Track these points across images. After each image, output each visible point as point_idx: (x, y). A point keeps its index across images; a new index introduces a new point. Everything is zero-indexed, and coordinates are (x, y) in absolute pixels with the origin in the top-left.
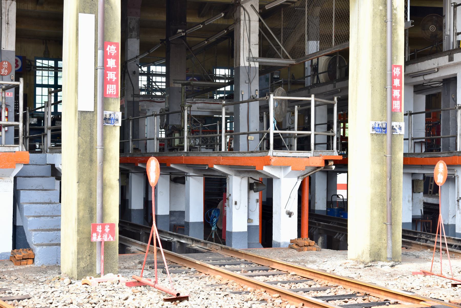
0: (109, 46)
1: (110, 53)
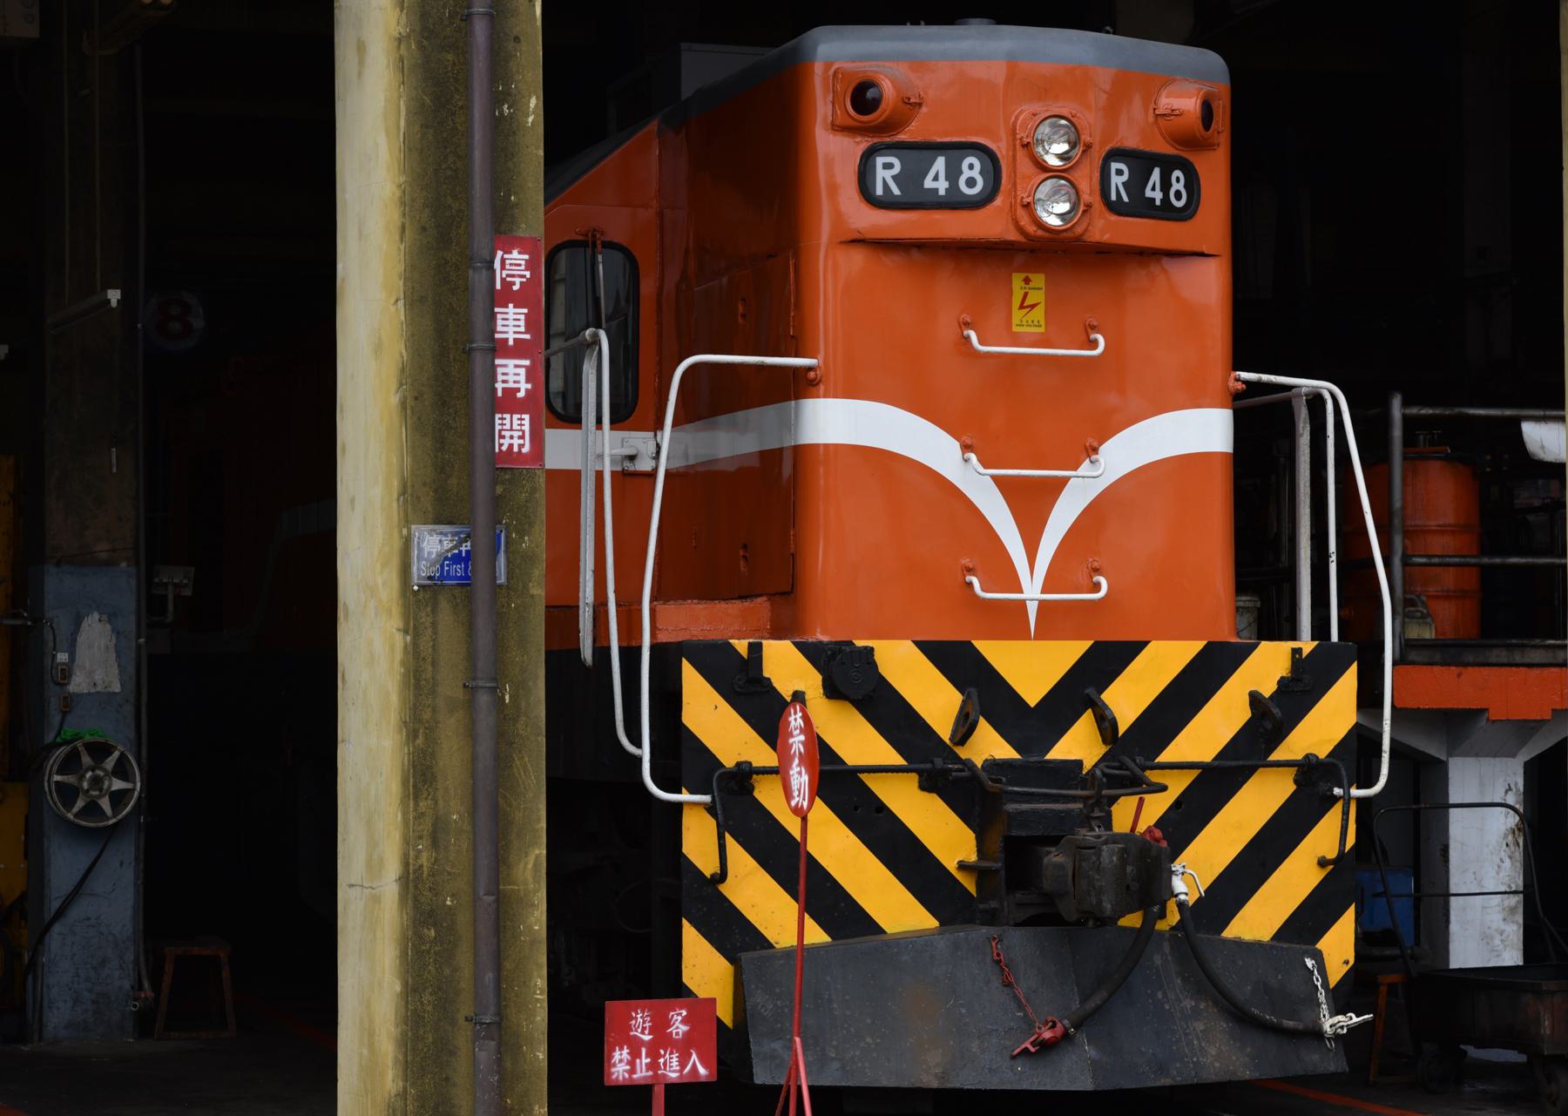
0: (500, 253)
1: (503, 280)
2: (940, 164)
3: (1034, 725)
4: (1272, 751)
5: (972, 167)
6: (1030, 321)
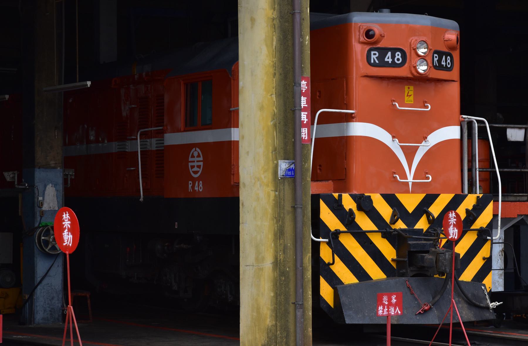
2: (389, 54)
3: (411, 218)
4: (471, 226)
5: (398, 55)
6: (409, 100)
